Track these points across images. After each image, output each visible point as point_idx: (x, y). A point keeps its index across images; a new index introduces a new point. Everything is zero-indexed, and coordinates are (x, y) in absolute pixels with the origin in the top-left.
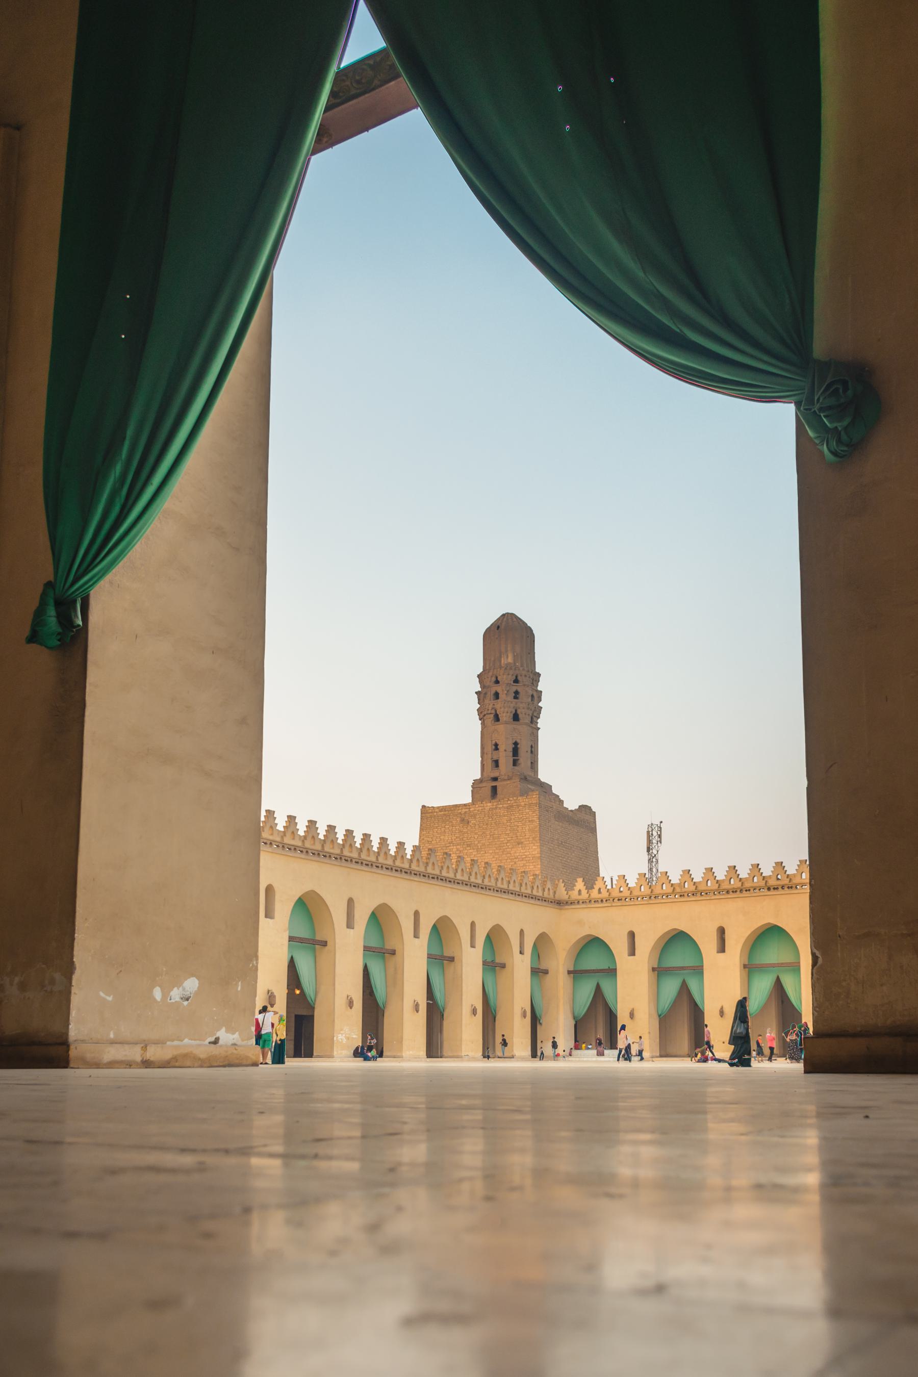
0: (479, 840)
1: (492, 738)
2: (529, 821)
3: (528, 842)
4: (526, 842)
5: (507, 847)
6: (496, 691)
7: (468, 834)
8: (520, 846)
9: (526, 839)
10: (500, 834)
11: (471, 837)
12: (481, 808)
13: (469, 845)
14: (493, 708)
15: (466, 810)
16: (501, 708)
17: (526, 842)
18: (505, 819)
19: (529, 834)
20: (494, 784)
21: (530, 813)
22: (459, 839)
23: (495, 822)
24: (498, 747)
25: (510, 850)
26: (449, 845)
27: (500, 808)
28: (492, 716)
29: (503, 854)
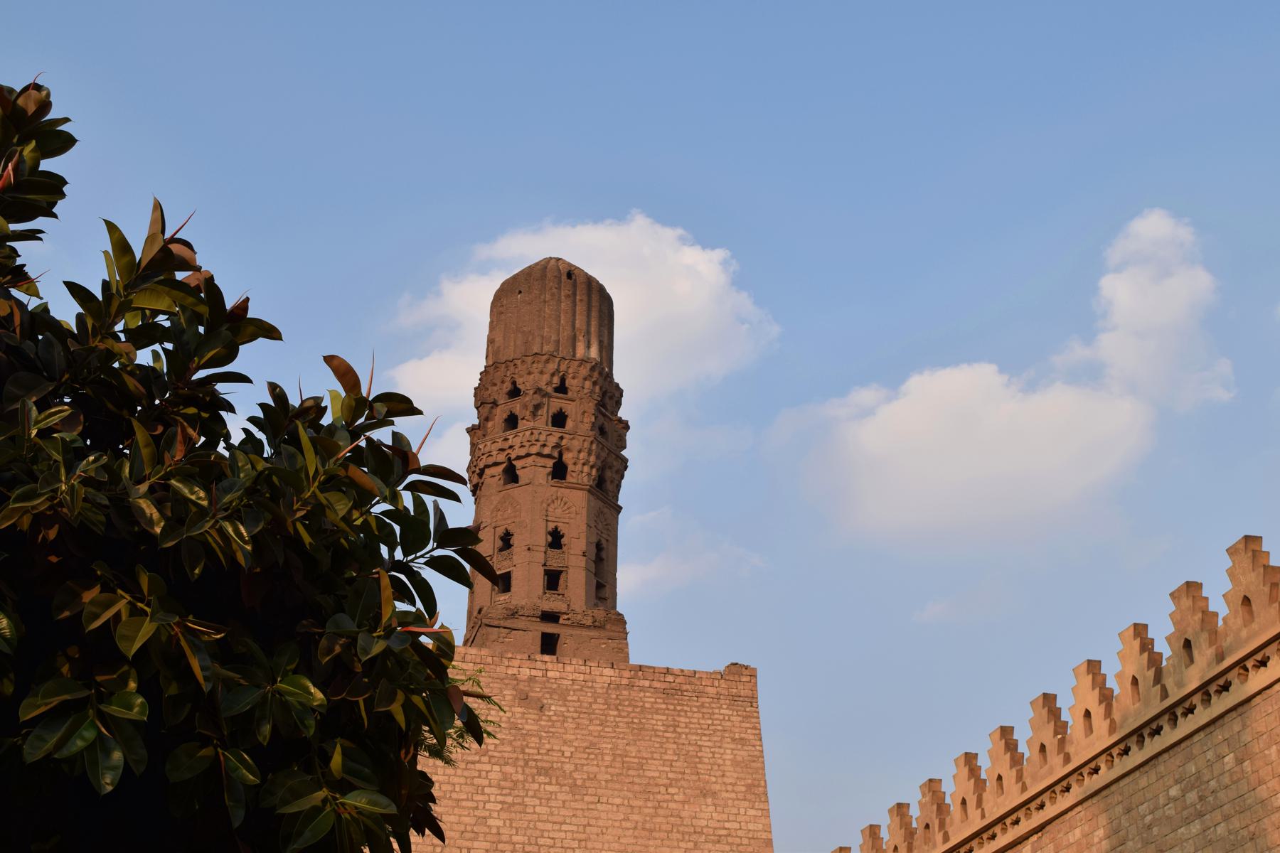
0: (577, 761)
1: (547, 516)
2: (734, 740)
3: (733, 795)
4: (725, 795)
5: (667, 797)
6: (561, 409)
7: (541, 738)
8: (709, 800)
9: (724, 783)
10: (646, 759)
11: (551, 750)
12: (582, 677)
13: (540, 771)
14: (557, 446)
15: (534, 673)
16: (580, 452)
17: (725, 795)
18: (658, 721)
19: (735, 775)
20: (550, 628)
21: (732, 718)
22: (509, 749)
23: (627, 723)
24: (564, 541)
25: (680, 806)
26: (477, 758)
27: (642, 689)
28: (550, 463)
29: (657, 815)
